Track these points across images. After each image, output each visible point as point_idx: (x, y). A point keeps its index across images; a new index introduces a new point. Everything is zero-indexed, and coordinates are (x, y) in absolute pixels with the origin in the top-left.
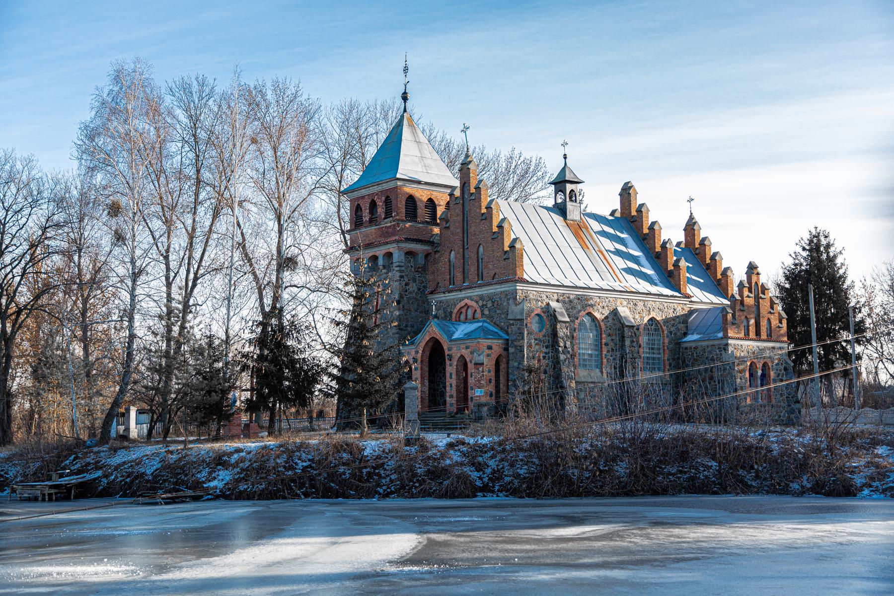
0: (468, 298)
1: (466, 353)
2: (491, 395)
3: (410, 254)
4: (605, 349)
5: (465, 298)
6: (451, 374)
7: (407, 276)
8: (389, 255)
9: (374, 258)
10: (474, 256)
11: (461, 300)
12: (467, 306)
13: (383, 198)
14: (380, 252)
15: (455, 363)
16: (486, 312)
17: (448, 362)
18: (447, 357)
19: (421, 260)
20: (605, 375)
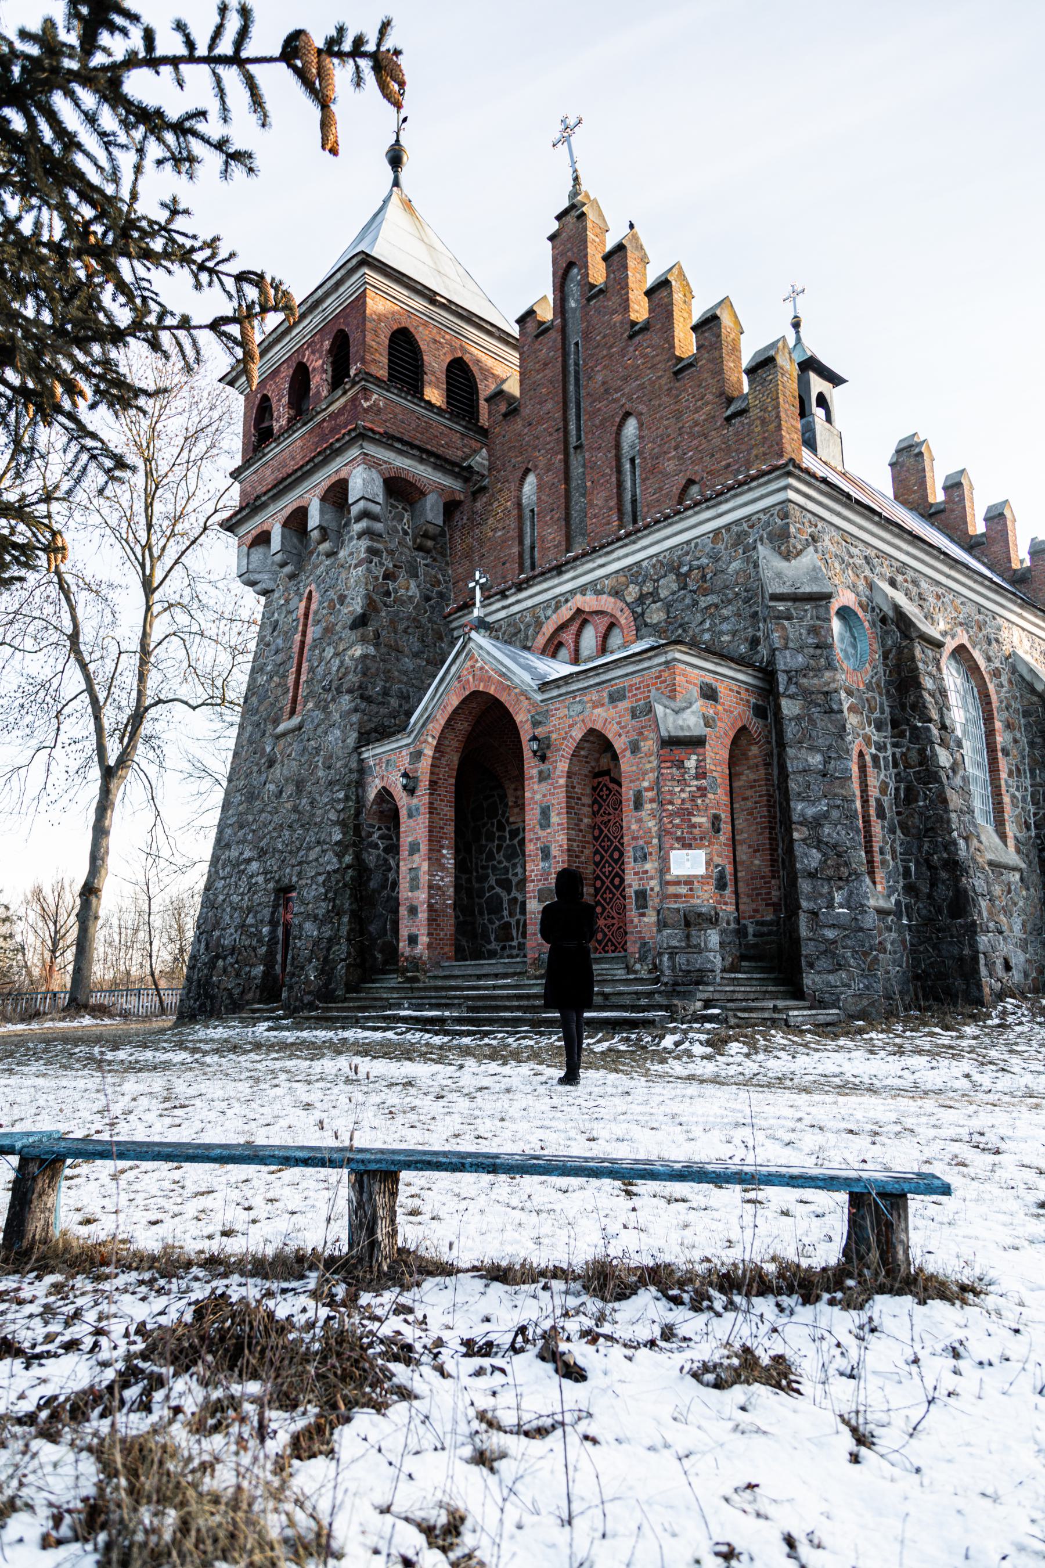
0: (582, 590)
1: (612, 721)
2: (721, 885)
3: (398, 489)
4: (1003, 764)
5: (572, 592)
6: (545, 813)
7: (391, 553)
8: (337, 496)
9: (297, 520)
10: (603, 459)
11: (557, 603)
12: (581, 618)
13: (327, 344)
14: (310, 495)
15: (562, 766)
16: (656, 615)
17: (532, 768)
18: (528, 749)
19: (432, 509)
20: (1011, 842)
